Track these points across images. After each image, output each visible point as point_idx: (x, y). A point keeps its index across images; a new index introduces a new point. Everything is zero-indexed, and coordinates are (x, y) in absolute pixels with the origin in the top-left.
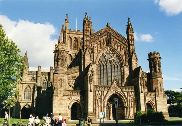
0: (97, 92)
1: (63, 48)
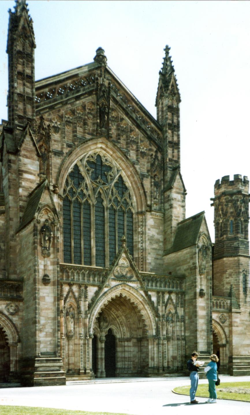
0: (66, 288)
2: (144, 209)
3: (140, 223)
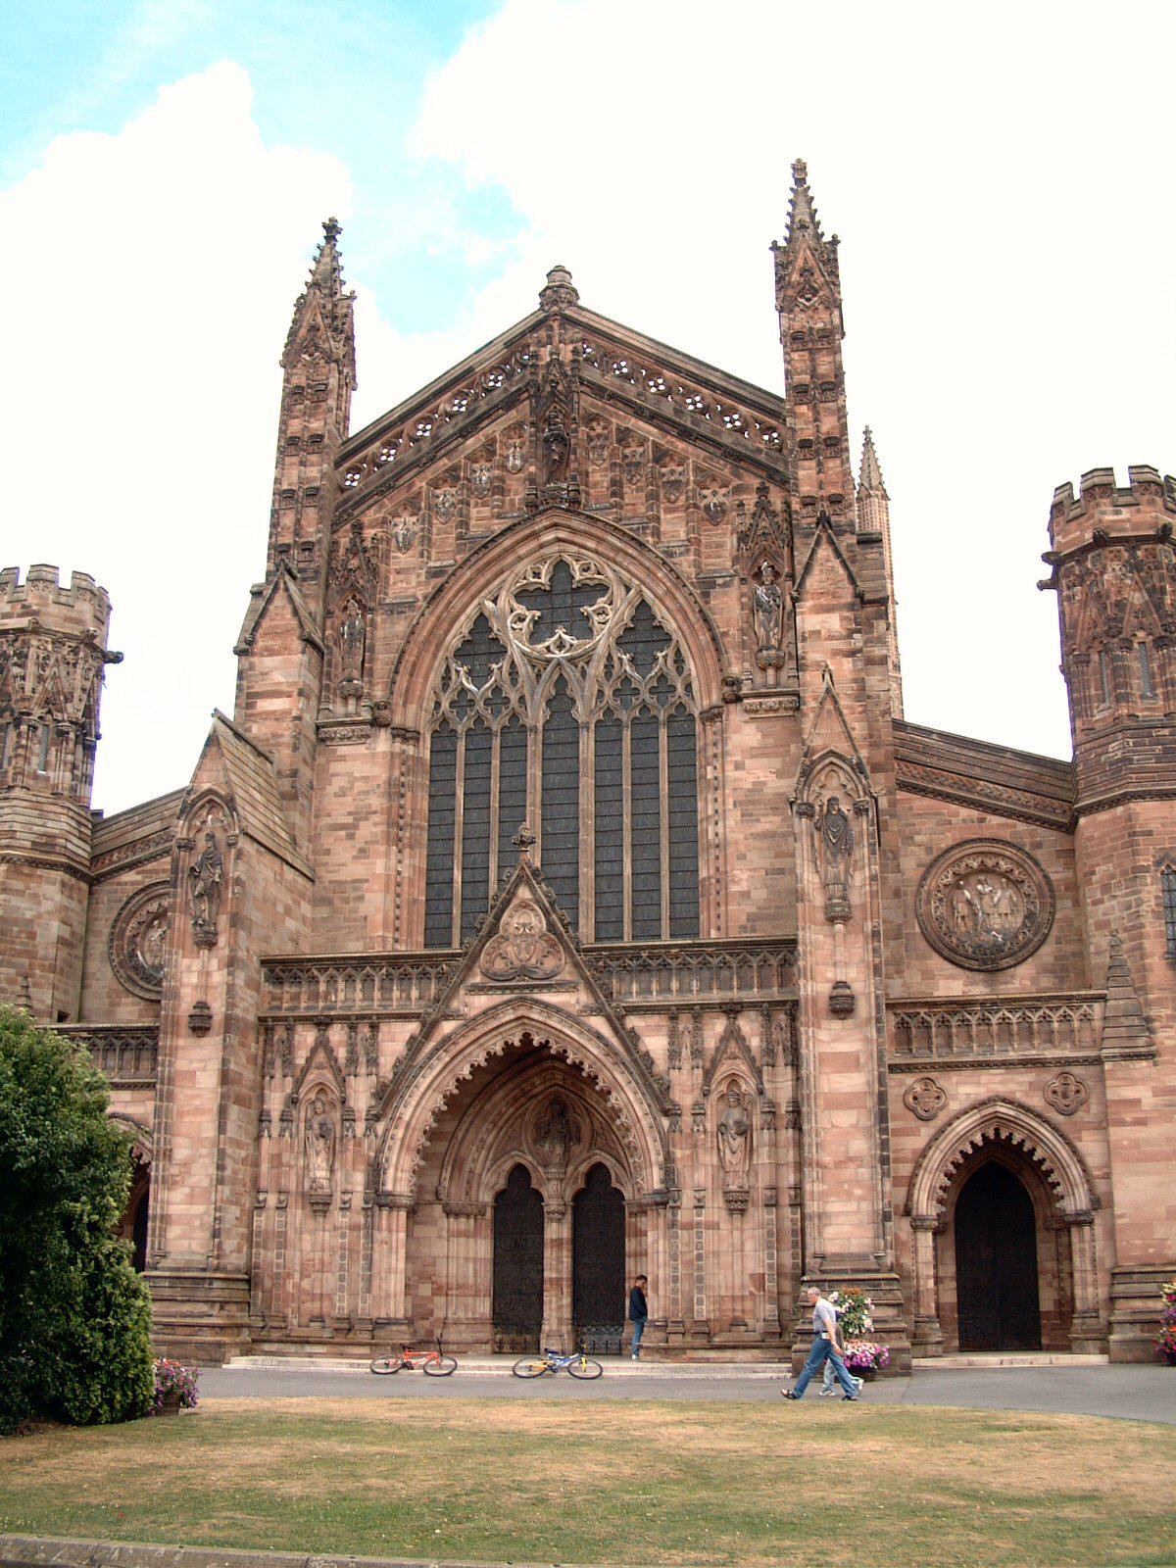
0: (307, 1036)
1: (27, 611)
2: (715, 699)
3: (711, 751)
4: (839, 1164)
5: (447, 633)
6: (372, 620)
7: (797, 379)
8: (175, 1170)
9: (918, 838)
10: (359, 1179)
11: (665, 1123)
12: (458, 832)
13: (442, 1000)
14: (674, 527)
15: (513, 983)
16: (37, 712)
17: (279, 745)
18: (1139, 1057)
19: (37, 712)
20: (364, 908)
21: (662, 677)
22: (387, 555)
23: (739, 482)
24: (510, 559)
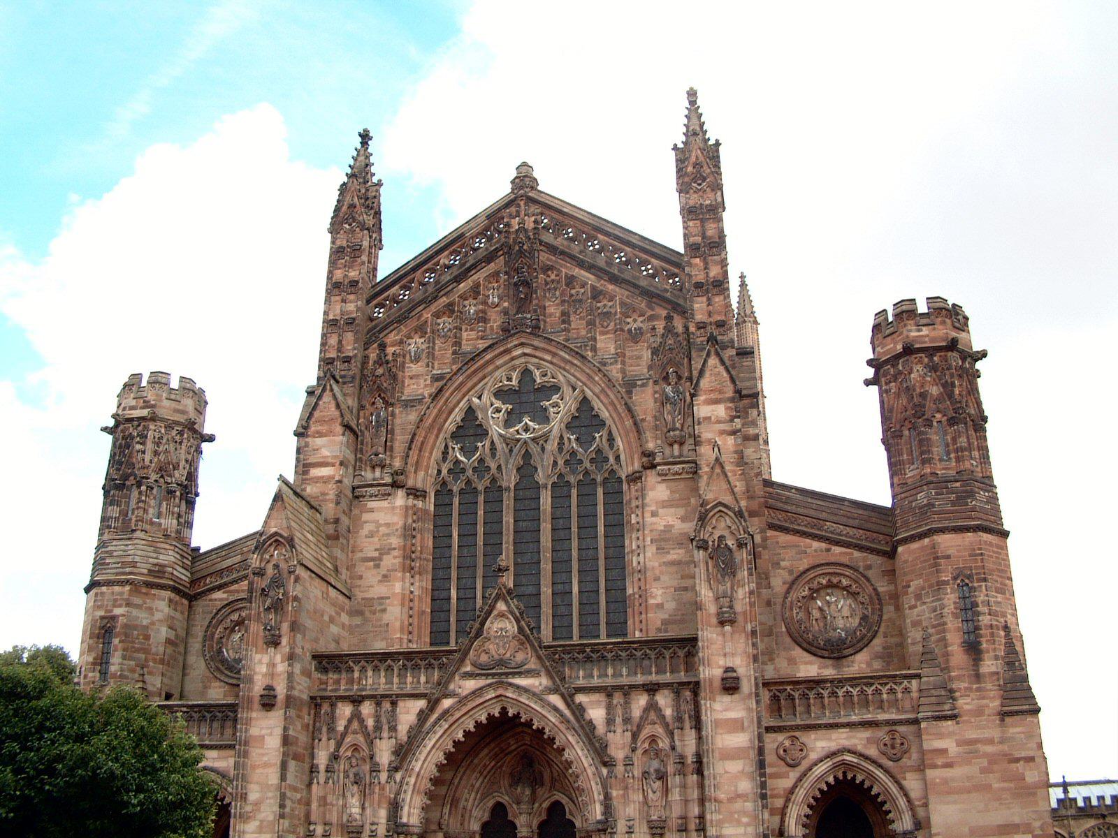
0: (345, 710)
1: (147, 405)
2: (637, 466)
3: (634, 503)
4: (730, 800)
5: (445, 421)
6: (393, 411)
7: (692, 239)
8: (248, 808)
9: (783, 564)
10: (383, 814)
11: (605, 771)
12: (454, 562)
13: (443, 684)
14: (606, 344)
15: (494, 671)
16: (154, 477)
17: (326, 501)
18: (946, 718)
19: (154, 477)
20: (387, 618)
21: (599, 451)
22: (403, 366)
23: (652, 313)
24: (491, 368)
